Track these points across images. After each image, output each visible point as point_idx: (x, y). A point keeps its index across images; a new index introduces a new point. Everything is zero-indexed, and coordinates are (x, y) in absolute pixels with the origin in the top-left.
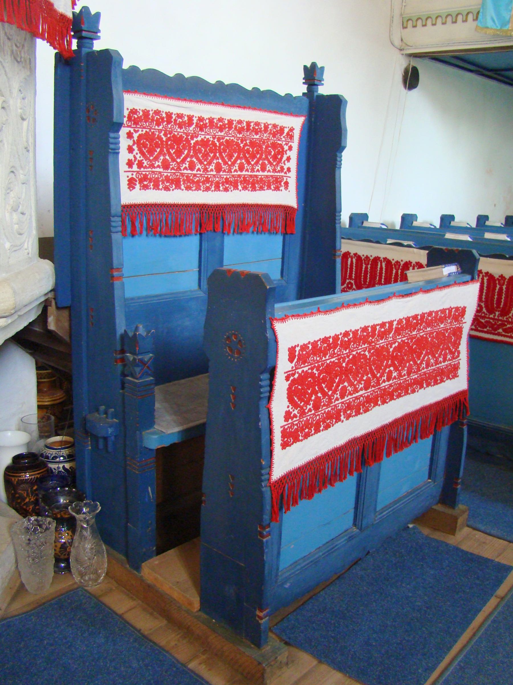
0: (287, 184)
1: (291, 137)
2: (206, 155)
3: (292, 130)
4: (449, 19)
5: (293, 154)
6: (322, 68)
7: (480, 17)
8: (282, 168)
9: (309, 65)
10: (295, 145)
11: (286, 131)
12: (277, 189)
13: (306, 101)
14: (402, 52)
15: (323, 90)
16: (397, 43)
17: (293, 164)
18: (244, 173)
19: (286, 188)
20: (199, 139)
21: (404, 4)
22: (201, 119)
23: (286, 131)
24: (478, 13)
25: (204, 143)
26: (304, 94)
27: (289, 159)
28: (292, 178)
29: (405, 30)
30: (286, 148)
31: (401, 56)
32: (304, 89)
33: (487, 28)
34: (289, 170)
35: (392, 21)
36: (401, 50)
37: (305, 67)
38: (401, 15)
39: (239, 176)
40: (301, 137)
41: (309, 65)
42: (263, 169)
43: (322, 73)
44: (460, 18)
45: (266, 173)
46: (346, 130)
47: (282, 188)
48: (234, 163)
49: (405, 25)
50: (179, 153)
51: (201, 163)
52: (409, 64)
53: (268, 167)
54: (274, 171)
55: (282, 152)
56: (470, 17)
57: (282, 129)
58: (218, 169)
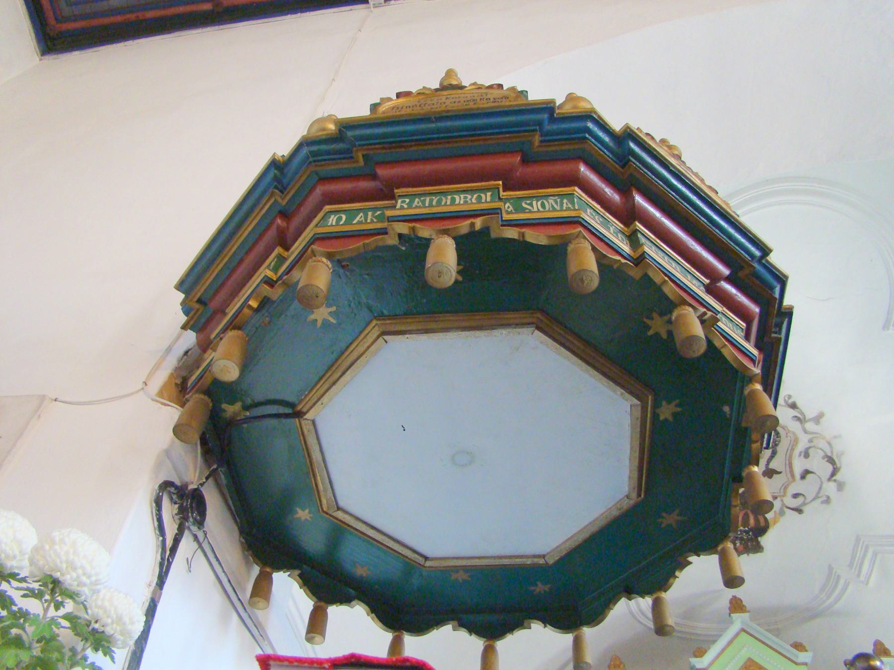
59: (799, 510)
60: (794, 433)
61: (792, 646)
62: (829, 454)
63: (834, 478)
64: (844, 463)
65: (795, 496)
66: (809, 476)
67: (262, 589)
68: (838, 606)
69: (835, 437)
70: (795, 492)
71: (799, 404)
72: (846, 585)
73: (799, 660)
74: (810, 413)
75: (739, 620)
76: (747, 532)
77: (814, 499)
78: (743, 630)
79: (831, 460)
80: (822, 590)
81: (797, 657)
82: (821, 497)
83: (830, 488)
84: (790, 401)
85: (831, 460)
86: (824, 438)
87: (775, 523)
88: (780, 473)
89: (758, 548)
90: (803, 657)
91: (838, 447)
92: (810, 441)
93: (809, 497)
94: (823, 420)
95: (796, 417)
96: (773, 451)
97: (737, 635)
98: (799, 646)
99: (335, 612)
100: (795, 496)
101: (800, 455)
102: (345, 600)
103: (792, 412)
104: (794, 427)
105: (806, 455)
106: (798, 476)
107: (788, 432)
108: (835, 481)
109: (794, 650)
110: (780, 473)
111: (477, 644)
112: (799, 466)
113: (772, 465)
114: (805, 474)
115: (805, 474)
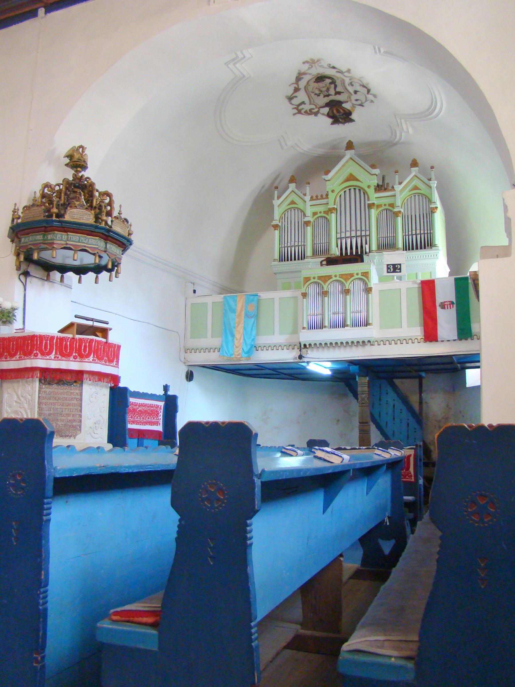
0: (160, 423)
1: (160, 408)
2: (140, 414)
3: (161, 406)
4: (207, 350)
5: (161, 414)
6: (169, 386)
7: (221, 350)
8: (158, 418)
9: (165, 385)
10: (162, 411)
11: (160, 406)
12: (157, 425)
13: (164, 397)
14: (185, 364)
15: (170, 393)
16: (183, 360)
17: (161, 417)
18: (149, 420)
19: (160, 425)
20: (139, 409)
21: (185, 342)
22: (139, 404)
23: (160, 406)
24: (220, 348)
25: (140, 411)
26: (163, 394)
27: (160, 416)
28: (161, 422)
29: (186, 354)
30: (160, 412)
31: (185, 366)
32: (163, 392)
33: (224, 356)
34: (160, 419)
35: (180, 351)
36: (184, 363)
37: (164, 386)
38: (184, 347)
39: (148, 421)
40: (163, 408)
41: (165, 385)
42: (154, 419)
43: (169, 387)
44: (212, 350)
45: (154, 420)
46: (178, 406)
47: (159, 425)
48: (147, 417)
49: (186, 352)
50: (134, 414)
51: (139, 416)
52: (189, 370)
53: (155, 418)
54: (157, 419)
55: (158, 414)
56: (216, 350)
57: (159, 406)
58: (143, 419)
59: (361, 105)
60: (341, 78)
61: (370, 166)
62: (362, 84)
63: (370, 93)
64: (370, 86)
65: (357, 100)
66: (358, 93)
67: (48, 276)
68: (401, 141)
69: (361, 78)
70: (357, 99)
71: (336, 66)
72: (401, 133)
73: (373, 173)
74: (344, 70)
75: (349, 154)
76: (343, 115)
77: (366, 101)
78: (351, 159)
79: (364, 86)
80: (392, 134)
81: (371, 171)
82: (368, 100)
83: (370, 97)
84: (331, 66)
85: (364, 86)
86: (356, 78)
87: (354, 110)
88: (343, 93)
89: (352, 121)
90: (377, 171)
91: (365, 82)
92: (350, 79)
93: (364, 100)
94: (351, 72)
95: (338, 72)
96: (334, 85)
97: (347, 162)
98: (373, 166)
99: (65, 275)
100: (357, 100)
101: (349, 85)
102: (67, 271)
103: (335, 70)
104: (339, 75)
105: (352, 85)
106: (353, 93)
107: (338, 78)
108: (371, 94)
109: (370, 168)
110: (343, 93)
111: (95, 275)
112: (351, 89)
113: (338, 90)
114: (356, 92)
115: (356, 92)
